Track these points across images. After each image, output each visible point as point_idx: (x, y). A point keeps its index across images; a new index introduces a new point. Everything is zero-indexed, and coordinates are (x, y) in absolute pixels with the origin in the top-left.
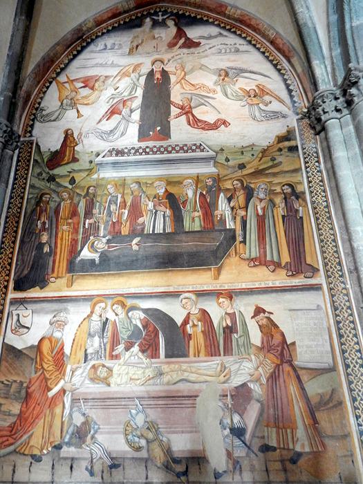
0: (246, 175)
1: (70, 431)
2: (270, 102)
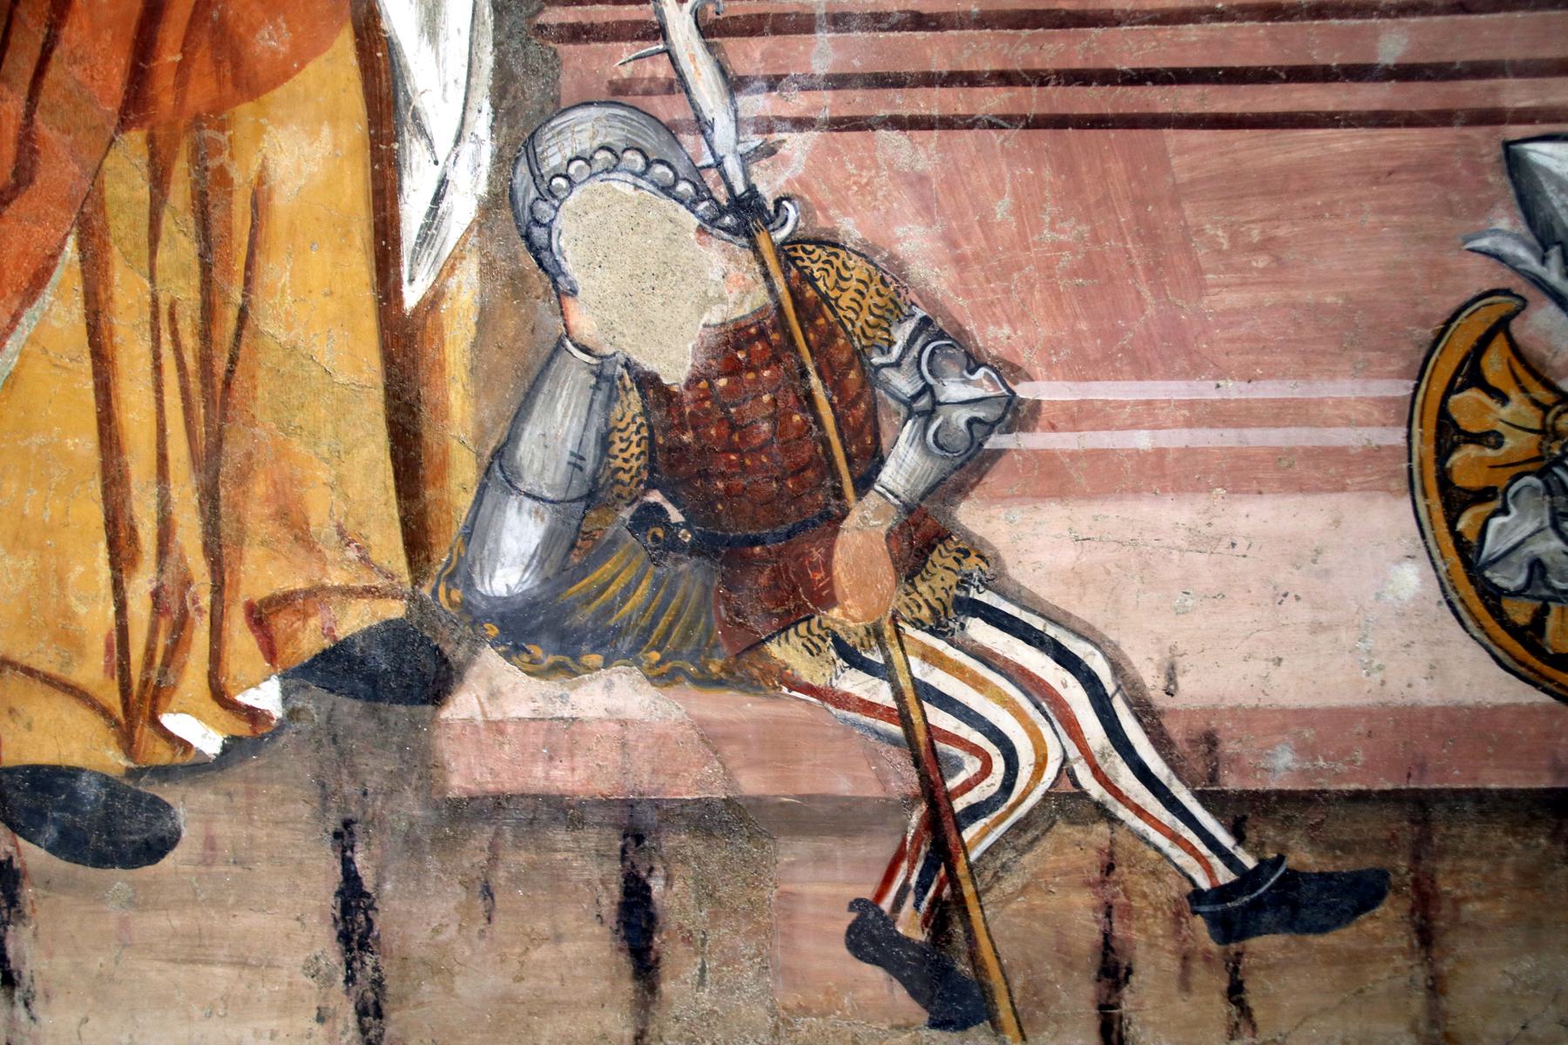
1: (556, 433)
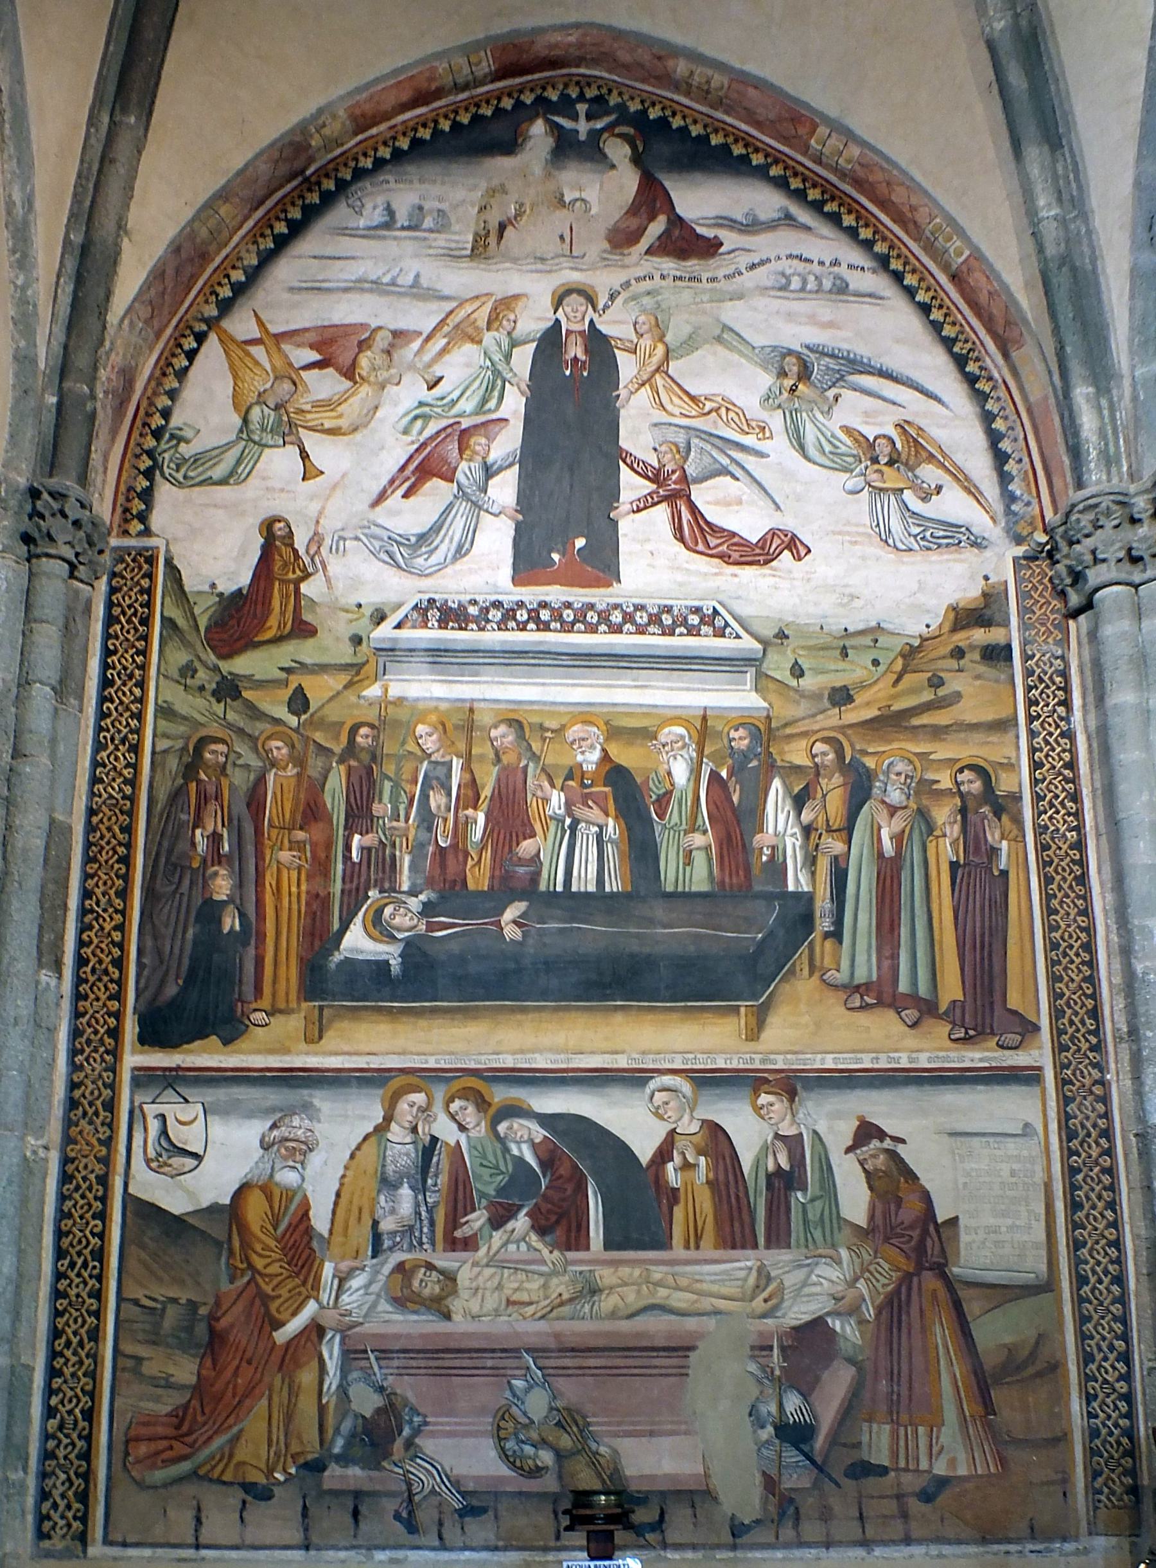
0: (851, 726)
1: (347, 1426)
2: (939, 489)
